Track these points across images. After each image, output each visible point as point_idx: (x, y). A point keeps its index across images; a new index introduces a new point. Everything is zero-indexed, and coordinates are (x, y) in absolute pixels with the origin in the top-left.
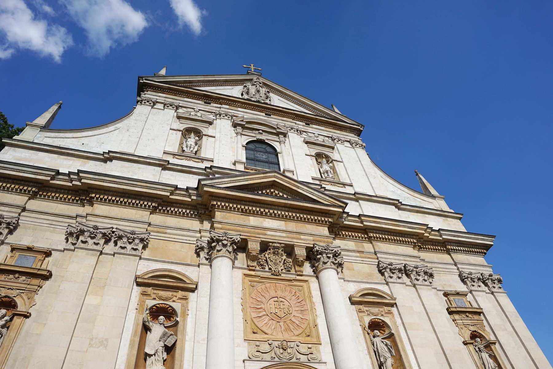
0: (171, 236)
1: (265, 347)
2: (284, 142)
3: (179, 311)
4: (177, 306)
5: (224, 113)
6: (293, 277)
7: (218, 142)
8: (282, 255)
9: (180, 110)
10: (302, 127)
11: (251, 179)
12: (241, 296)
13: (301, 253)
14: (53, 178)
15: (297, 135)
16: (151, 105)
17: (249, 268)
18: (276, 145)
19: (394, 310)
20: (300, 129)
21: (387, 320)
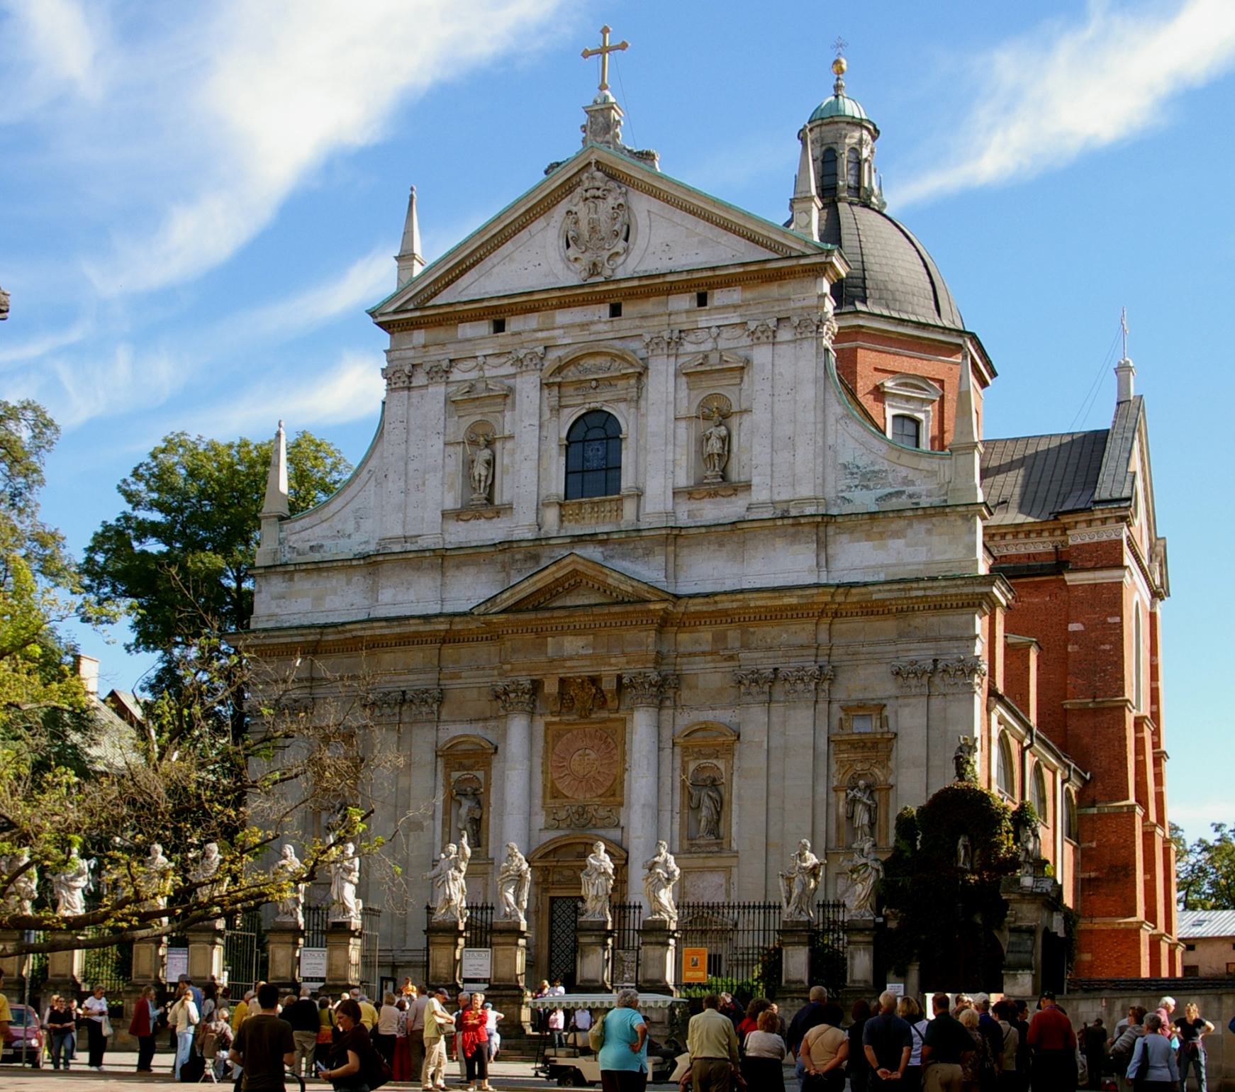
0: (468, 681)
1: (562, 814)
2: (637, 401)
3: (482, 781)
4: (480, 774)
5: (525, 351)
6: (603, 715)
7: (518, 457)
8: (590, 689)
9: (456, 375)
10: (683, 318)
11: (539, 581)
12: (541, 754)
13: (608, 685)
14: (321, 634)
15: (668, 356)
16: (405, 385)
17: (552, 714)
18: (621, 412)
19: (737, 745)
20: (676, 334)
21: (721, 764)
